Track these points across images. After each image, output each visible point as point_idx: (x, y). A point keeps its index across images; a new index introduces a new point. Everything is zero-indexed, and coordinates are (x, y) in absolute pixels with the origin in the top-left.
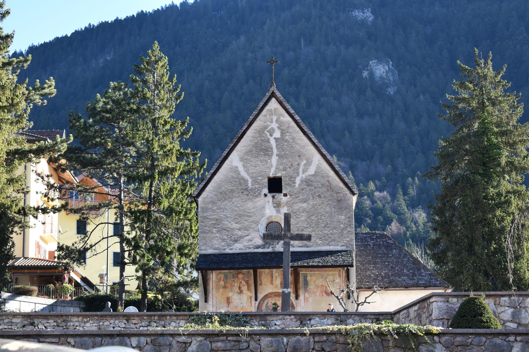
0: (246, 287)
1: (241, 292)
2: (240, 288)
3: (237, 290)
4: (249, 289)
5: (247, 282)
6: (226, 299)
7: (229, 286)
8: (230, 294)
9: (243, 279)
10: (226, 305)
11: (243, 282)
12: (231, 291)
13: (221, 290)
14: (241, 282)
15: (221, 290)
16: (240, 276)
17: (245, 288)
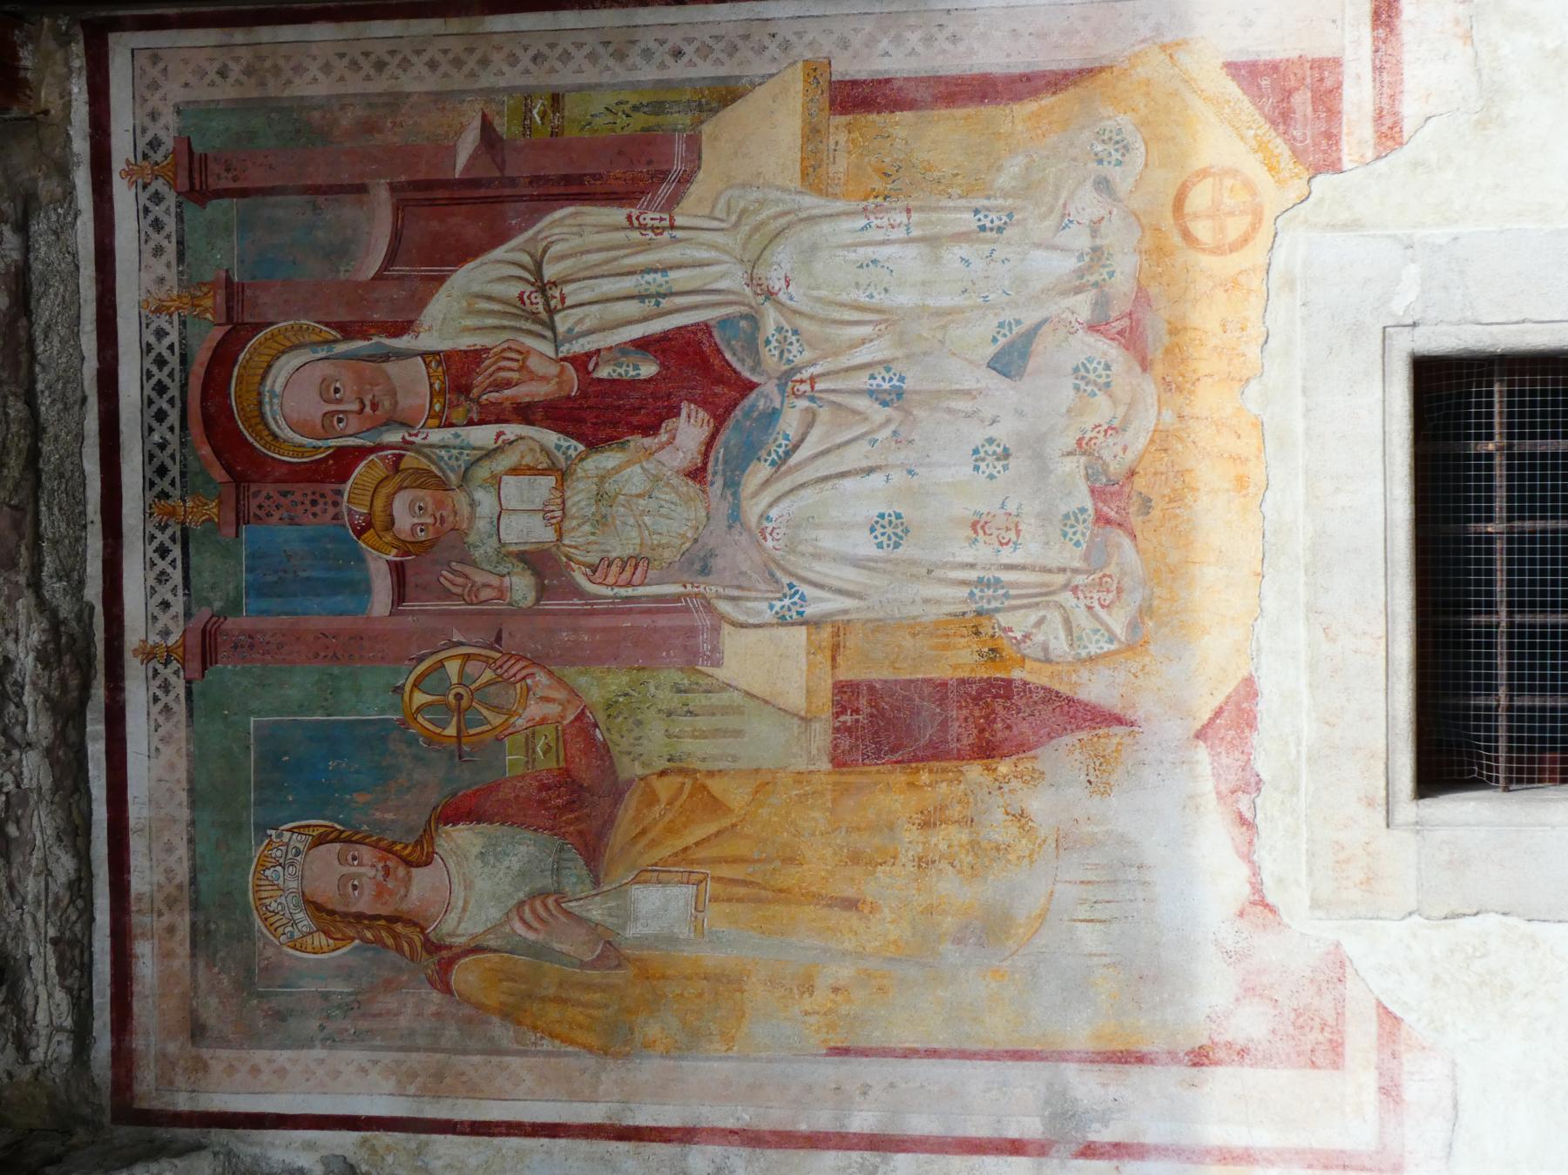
0: (575, 235)
1: (697, 374)
2: (601, 412)
3: (642, 490)
4: (636, 168)
5: (455, 211)
6: (891, 795)
7: (540, 705)
8: (768, 662)
9: (376, 317)
10: (1050, 789)
11: (453, 315)
12: (671, 637)
13: (656, 909)
14: (459, 376)
15: (656, 909)
16: (294, 392)
17: (605, 279)
